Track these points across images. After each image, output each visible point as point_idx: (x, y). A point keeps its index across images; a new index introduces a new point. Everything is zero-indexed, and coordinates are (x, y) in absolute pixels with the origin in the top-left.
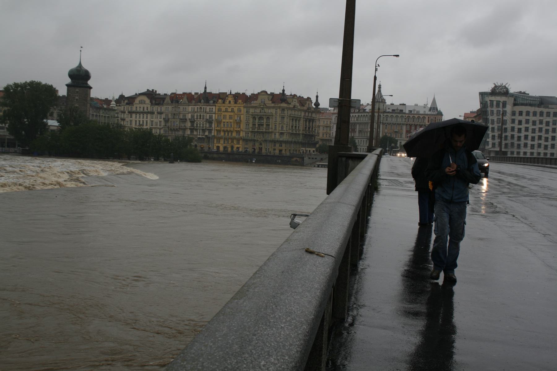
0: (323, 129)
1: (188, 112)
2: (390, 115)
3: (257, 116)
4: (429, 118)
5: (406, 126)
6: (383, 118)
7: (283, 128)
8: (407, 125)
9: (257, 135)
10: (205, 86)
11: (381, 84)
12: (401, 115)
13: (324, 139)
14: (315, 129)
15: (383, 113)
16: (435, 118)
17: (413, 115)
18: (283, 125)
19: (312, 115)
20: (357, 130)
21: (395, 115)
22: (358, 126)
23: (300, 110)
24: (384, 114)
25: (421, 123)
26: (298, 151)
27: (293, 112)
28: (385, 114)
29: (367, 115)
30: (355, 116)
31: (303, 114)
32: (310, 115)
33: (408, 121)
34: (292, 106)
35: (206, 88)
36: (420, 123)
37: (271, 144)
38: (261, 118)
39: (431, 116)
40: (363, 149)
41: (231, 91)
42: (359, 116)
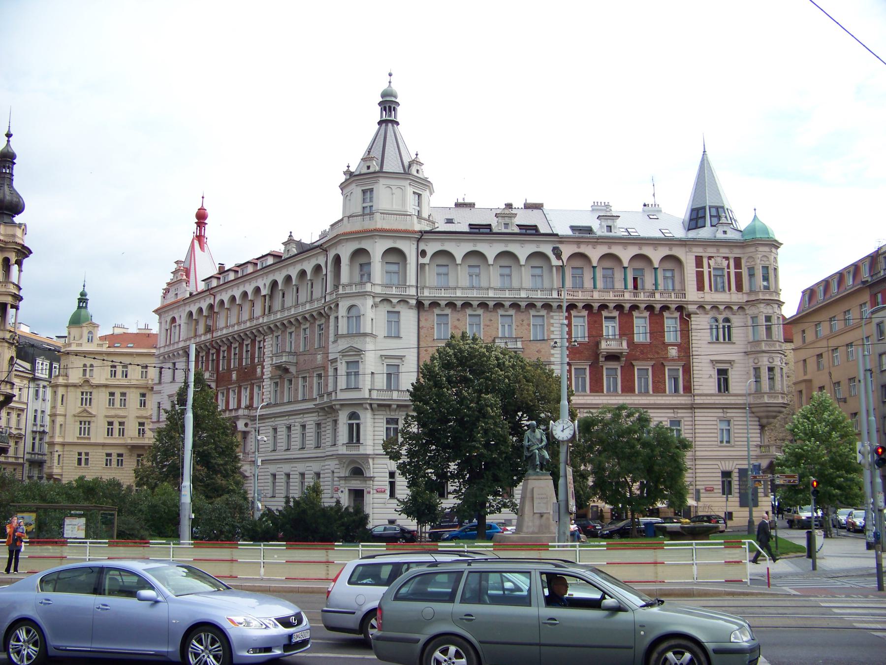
2: (459, 250)
4: (699, 261)
5: (569, 318)
6: (421, 267)
8: (572, 307)
11: (395, 87)
12: (531, 248)
13: (142, 447)
15: (419, 240)
16: (738, 262)
17: (603, 250)
20: (268, 371)
21: (491, 250)
22: (269, 345)
24: (422, 246)
25: (658, 297)
28: (431, 248)
29: (318, 268)
30: (257, 290)
33: (579, 286)
36: (653, 294)
39: (711, 251)
40: (303, 475)
42: (274, 284)
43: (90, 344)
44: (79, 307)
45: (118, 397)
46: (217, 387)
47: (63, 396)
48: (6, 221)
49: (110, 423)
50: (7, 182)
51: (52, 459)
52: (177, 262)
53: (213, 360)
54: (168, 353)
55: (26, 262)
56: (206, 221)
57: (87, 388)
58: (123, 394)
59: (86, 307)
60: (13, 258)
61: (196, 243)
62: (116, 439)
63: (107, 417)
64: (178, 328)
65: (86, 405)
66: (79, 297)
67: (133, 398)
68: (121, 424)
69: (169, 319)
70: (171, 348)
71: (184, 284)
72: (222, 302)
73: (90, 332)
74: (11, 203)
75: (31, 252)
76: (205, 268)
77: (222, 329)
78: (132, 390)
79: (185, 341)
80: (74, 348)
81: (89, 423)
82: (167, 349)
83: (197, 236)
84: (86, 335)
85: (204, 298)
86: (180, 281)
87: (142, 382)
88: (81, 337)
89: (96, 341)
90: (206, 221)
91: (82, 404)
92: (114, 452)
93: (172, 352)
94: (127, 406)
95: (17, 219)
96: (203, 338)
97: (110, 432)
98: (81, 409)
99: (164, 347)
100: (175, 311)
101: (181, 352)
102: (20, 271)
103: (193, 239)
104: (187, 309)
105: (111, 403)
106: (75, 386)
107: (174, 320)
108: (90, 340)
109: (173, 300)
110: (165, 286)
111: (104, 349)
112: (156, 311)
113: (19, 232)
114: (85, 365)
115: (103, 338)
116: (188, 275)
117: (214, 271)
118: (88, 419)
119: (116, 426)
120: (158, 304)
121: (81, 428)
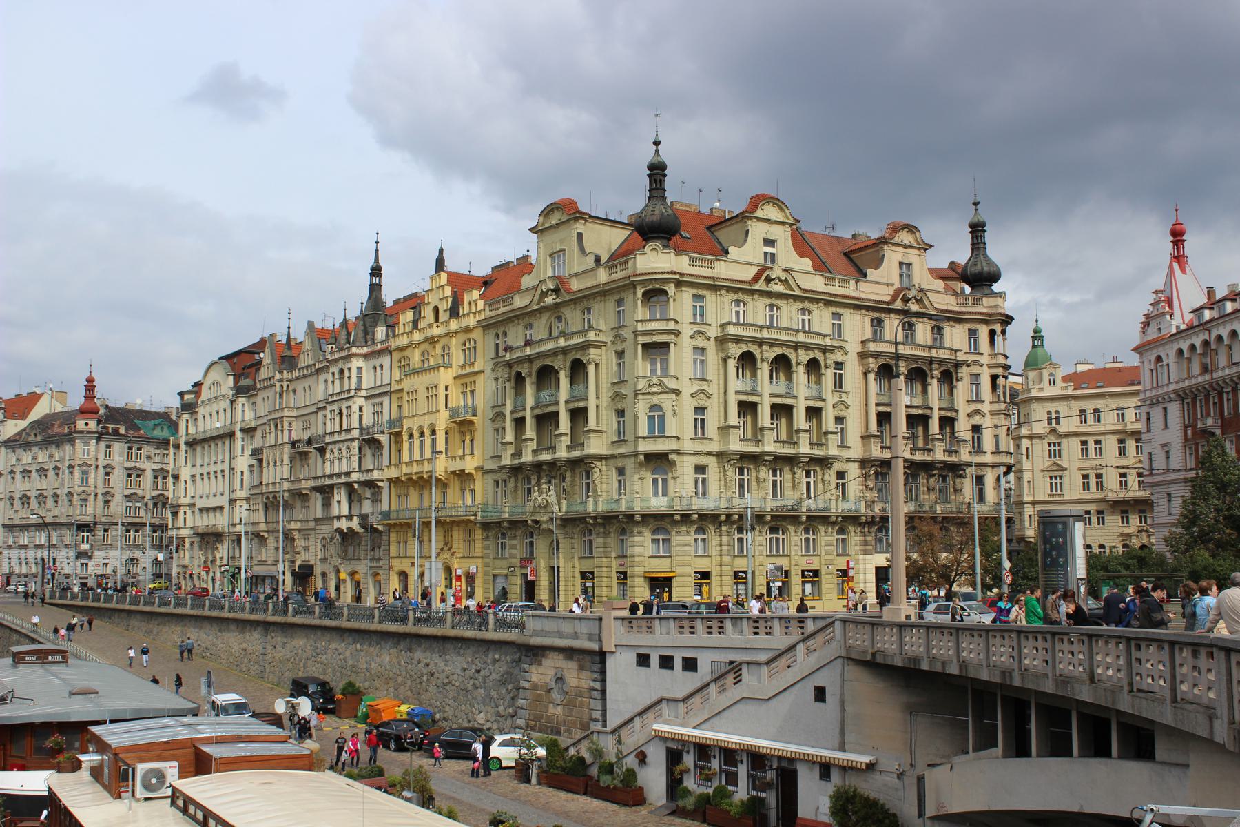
0: (1123, 452)
1: (313, 409)
3: (527, 365)
7: (662, 418)
9: (516, 487)
10: (371, 262)
13: (1124, 502)
14: (977, 429)
18: (656, 400)
19: (938, 331)
23: (809, 298)
26: (829, 581)
27: (757, 311)
31: (856, 327)
32: (923, 331)
34: (748, 274)
35: (376, 271)
37: (601, 540)
38: (546, 375)
41: (441, 251)
43: (1052, 387)
44: (1034, 346)
45: (1091, 446)
46: (1223, 434)
47: (1027, 449)
48: (986, 292)
49: (1085, 477)
50: (981, 252)
51: (1022, 521)
52: (1156, 292)
53: (1215, 403)
54: (1156, 397)
55: (1009, 328)
56: (1184, 238)
57: (1056, 439)
58: (1097, 442)
59: (1042, 345)
60: (998, 328)
61: (1175, 265)
62: (1094, 494)
63: (1080, 469)
64: (1166, 367)
65: (1055, 457)
66: (1033, 334)
67: (1110, 444)
68: (1099, 476)
69: (1153, 358)
70: (1160, 391)
71: (1168, 317)
72: (1220, 338)
73: (1051, 374)
74: (989, 273)
75: (1012, 319)
76: (1190, 295)
77: (1223, 369)
78: (1107, 436)
79: (1177, 382)
80: (1034, 394)
81: (1061, 477)
82: (1154, 393)
83: (1175, 257)
84: (1046, 378)
85: (1197, 334)
86: (1163, 314)
87: (1119, 427)
88: (1041, 380)
89: (1059, 383)
90: (1184, 238)
91: (1050, 457)
92: (1092, 508)
93: (1162, 395)
94: (1104, 455)
95: (996, 287)
96: (1200, 379)
97: (1086, 487)
98: (1050, 463)
99: (1151, 390)
100: (1161, 349)
101: (1173, 396)
102: (1004, 340)
103: (1171, 264)
104: (1176, 346)
105: (1085, 452)
106: (1040, 437)
107: (1159, 359)
108: (1052, 383)
109: (1156, 336)
110: (1143, 319)
111: (1070, 391)
112: (1135, 350)
113: (999, 301)
114: (1049, 412)
115: (1065, 379)
116: (1171, 306)
117: (1203, 300)
118: (1060, 473)
119: (1093, 480)
120: (1137, 340)
121: (1051, 484)
